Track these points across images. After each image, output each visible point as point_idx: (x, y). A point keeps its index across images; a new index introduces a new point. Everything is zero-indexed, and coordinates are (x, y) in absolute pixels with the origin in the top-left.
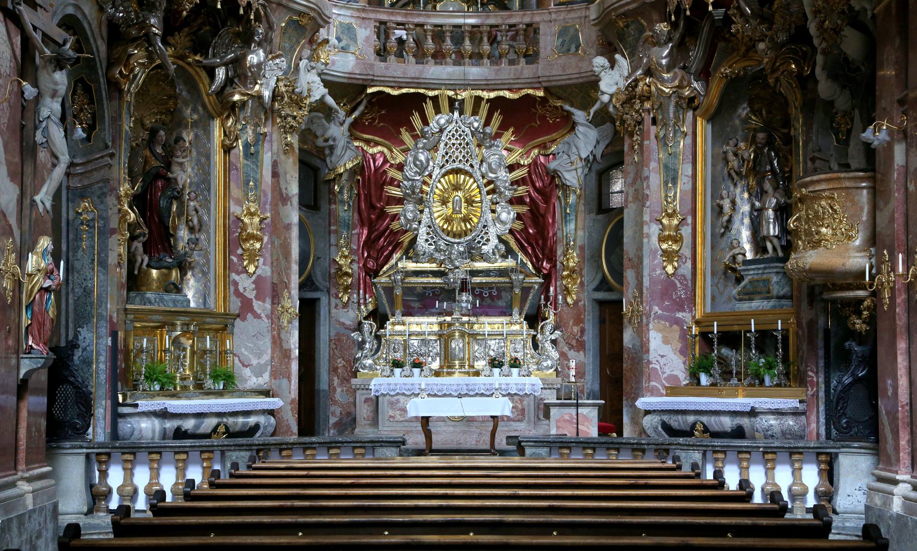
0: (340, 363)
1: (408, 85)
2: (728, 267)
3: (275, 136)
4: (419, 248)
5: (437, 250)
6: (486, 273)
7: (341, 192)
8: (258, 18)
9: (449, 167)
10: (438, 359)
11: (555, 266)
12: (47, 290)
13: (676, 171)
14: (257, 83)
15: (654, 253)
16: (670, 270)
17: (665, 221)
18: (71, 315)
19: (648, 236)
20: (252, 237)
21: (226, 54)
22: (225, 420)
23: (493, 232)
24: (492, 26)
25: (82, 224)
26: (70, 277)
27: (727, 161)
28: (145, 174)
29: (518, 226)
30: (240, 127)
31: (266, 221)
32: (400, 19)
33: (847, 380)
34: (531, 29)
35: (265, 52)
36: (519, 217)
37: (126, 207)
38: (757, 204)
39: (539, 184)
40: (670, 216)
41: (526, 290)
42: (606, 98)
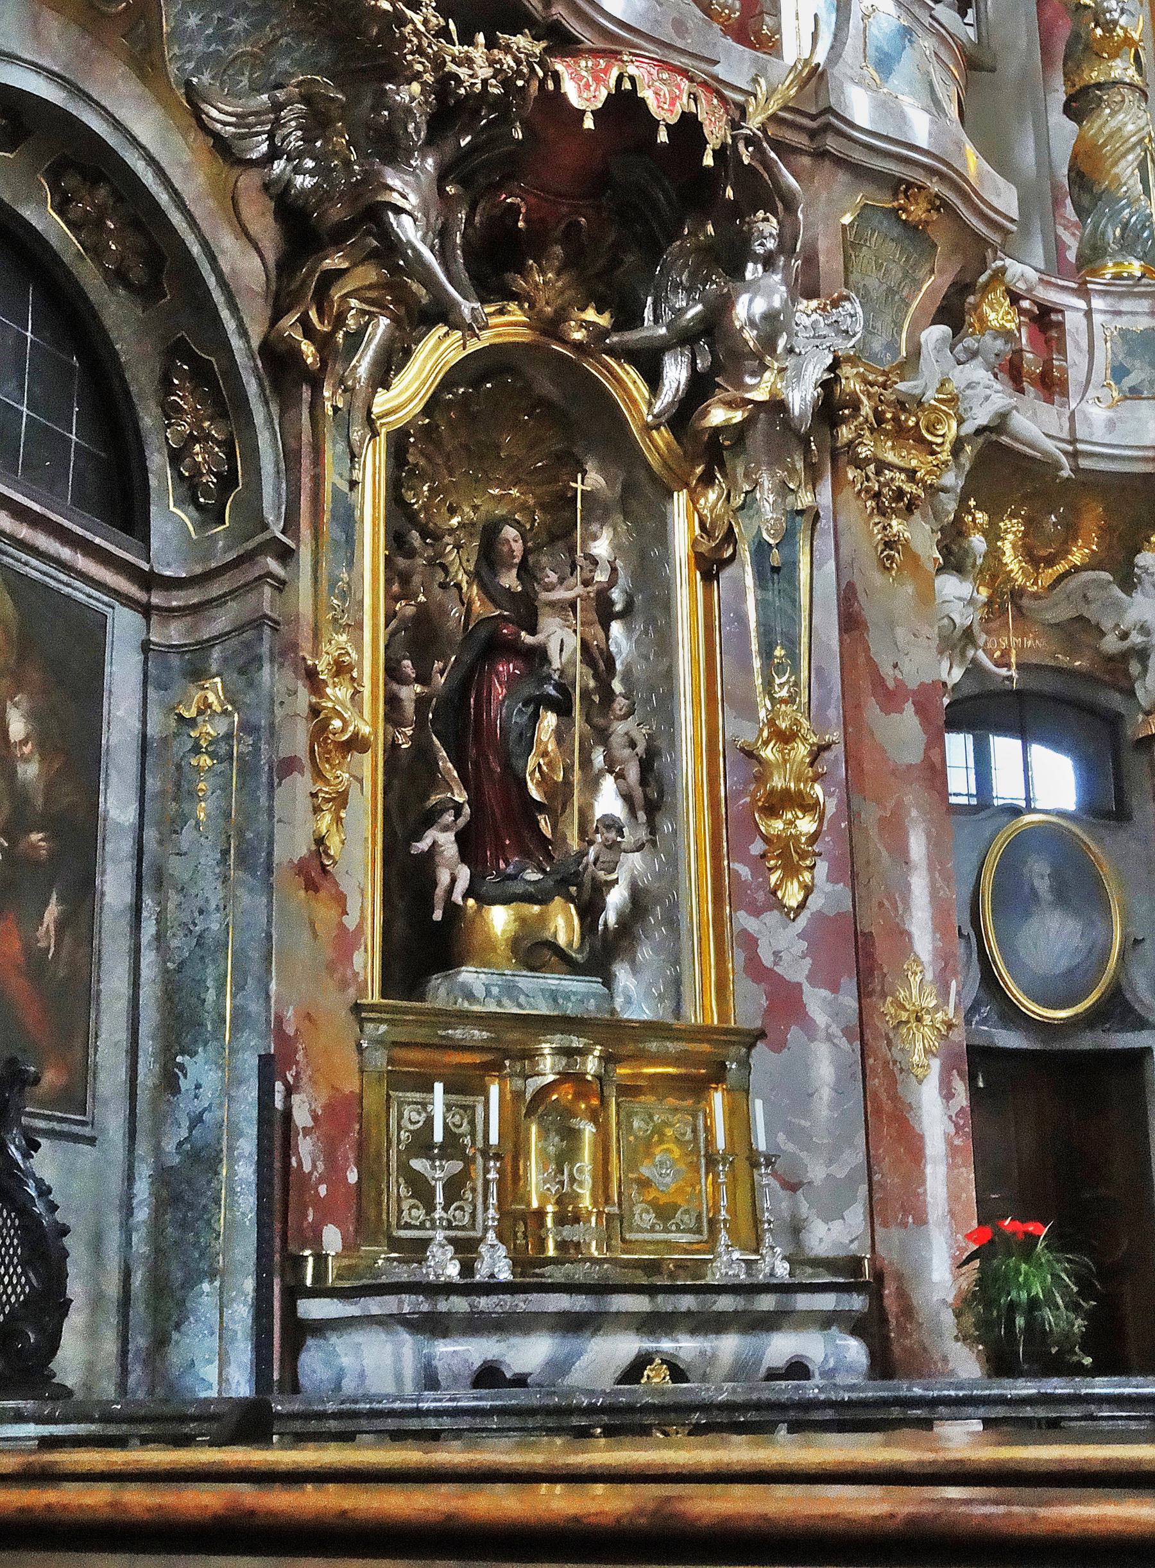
14: (764, 368)
22: (666, 1345)
25: (196, 750)
26: (148, 901)
30: (738, 501)
31: (826, 755)
35: (785, 281)
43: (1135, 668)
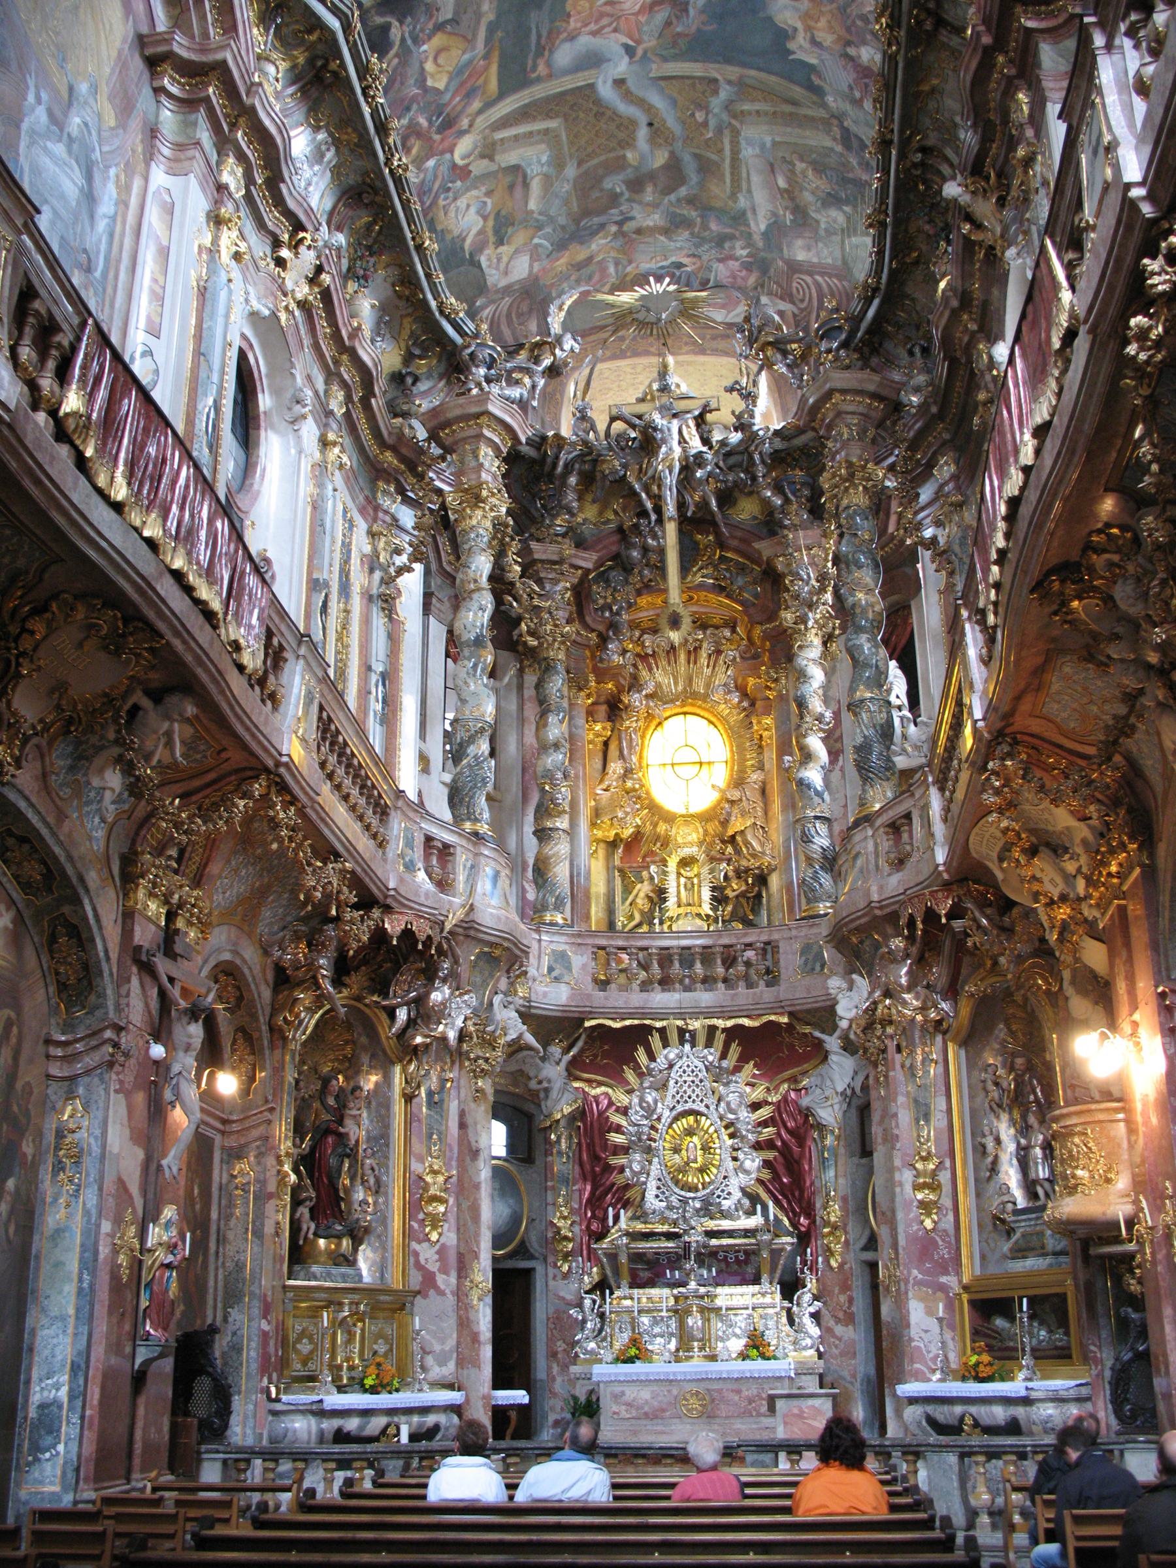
0: (560, 1346)
1: (631, 1016)
2: (996, 1218)
3: (462, 1082)
4: (648, 1205)
5: (670, 1208)
6: (730, 1234)
7: (558, 1141)
8: (441, 952)
9: (680, 1108)
10: (674, 1340)
11: (814, 1222)
12: (169, 1266)
13: (927, 1106)
15: (908, 1204)
16: (928, 1224)
17: (919, 1166)
18: (220, 1293)
19: (901, 1184)
20: (435, 1199)
21: (409, 992)
23: (735, 1184)
24: (725, 946)
27: (987, 1092)
28: (316, 1129)
29: (766, 1175)
32: (620, 943)
33: (1127, 1356)
34: (769, 948)
36: (767, 1164)
37: (287, 1168)
38: (1023, 1141)
39: (791, 1124)
40: (924, 1159)
41: (776, 1253)
42: (844, 1024)
43: (542, 1095)
